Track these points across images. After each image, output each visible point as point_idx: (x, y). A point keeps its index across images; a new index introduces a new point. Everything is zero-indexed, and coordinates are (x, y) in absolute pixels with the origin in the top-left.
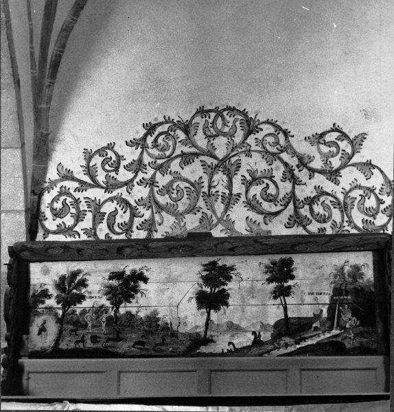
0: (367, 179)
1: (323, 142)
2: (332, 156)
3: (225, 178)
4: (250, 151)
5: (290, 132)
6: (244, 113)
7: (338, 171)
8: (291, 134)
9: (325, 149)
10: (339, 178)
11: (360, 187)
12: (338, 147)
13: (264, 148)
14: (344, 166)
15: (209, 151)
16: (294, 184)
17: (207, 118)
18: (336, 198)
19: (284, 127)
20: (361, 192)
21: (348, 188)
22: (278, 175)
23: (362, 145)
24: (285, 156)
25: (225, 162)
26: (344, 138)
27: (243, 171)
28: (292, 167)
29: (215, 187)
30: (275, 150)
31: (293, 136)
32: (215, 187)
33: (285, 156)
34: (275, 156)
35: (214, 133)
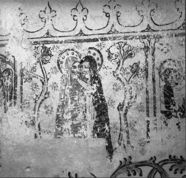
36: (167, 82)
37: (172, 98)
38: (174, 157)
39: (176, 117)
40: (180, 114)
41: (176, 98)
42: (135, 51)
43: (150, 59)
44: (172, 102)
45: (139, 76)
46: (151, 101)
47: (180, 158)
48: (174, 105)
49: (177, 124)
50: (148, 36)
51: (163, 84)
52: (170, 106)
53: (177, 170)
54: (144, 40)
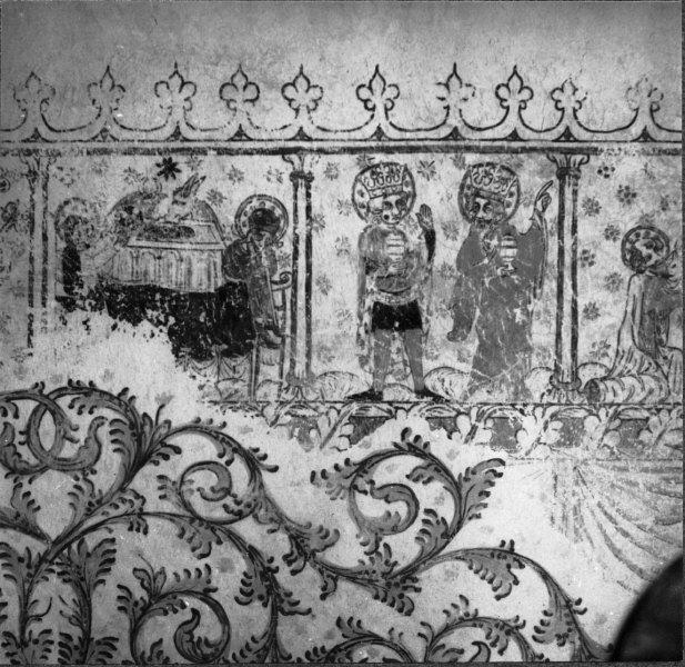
0: (498, 598)
1: (368, 487)
2: (395, 530)
3: (68, 592)
4: (142, 514)
5: (265, 457)
6: (123, 401)
7: (410, 574)
8: (268, 462)
9: (372, 508)
10: (411, 595)
11: (475, 620)
12: (413, 501)
13: (187, 505)
14: (428, 557)
15: (18, 515)
16: (276, 611)
17: (10, 418)
18: (403, 652)
19: (247, 443)
20: (479, 634)
21: (438, 622)
22: (227, 585)
23: (488, 494)
24: (248, 529)
25: (68, 545)
26: (434, 474)
27: (122, 571)
28: (271, 560)
29: (39, 618)
30: (220, 514)
31: (275, 469)
32: (39, 618)
33: (248, 529)
34: (220, 531)
35: (33, 461)
36: (69, 242)
37: (78, 273)
38: (78, 382)
39: (83, 309)
40: (90, 304)
41: (84, 273)
42: (11, 180)
43: (38, 197)
44: (78, 279)
45: (18, 228)
46: (38, 278)
47: (87, 385)
48: (81, 286)
49: (85, 323)
50: (36, 151)
51: (62, 245)
52: (73, 289)
53: (83, 406)
54: (28, 158)
